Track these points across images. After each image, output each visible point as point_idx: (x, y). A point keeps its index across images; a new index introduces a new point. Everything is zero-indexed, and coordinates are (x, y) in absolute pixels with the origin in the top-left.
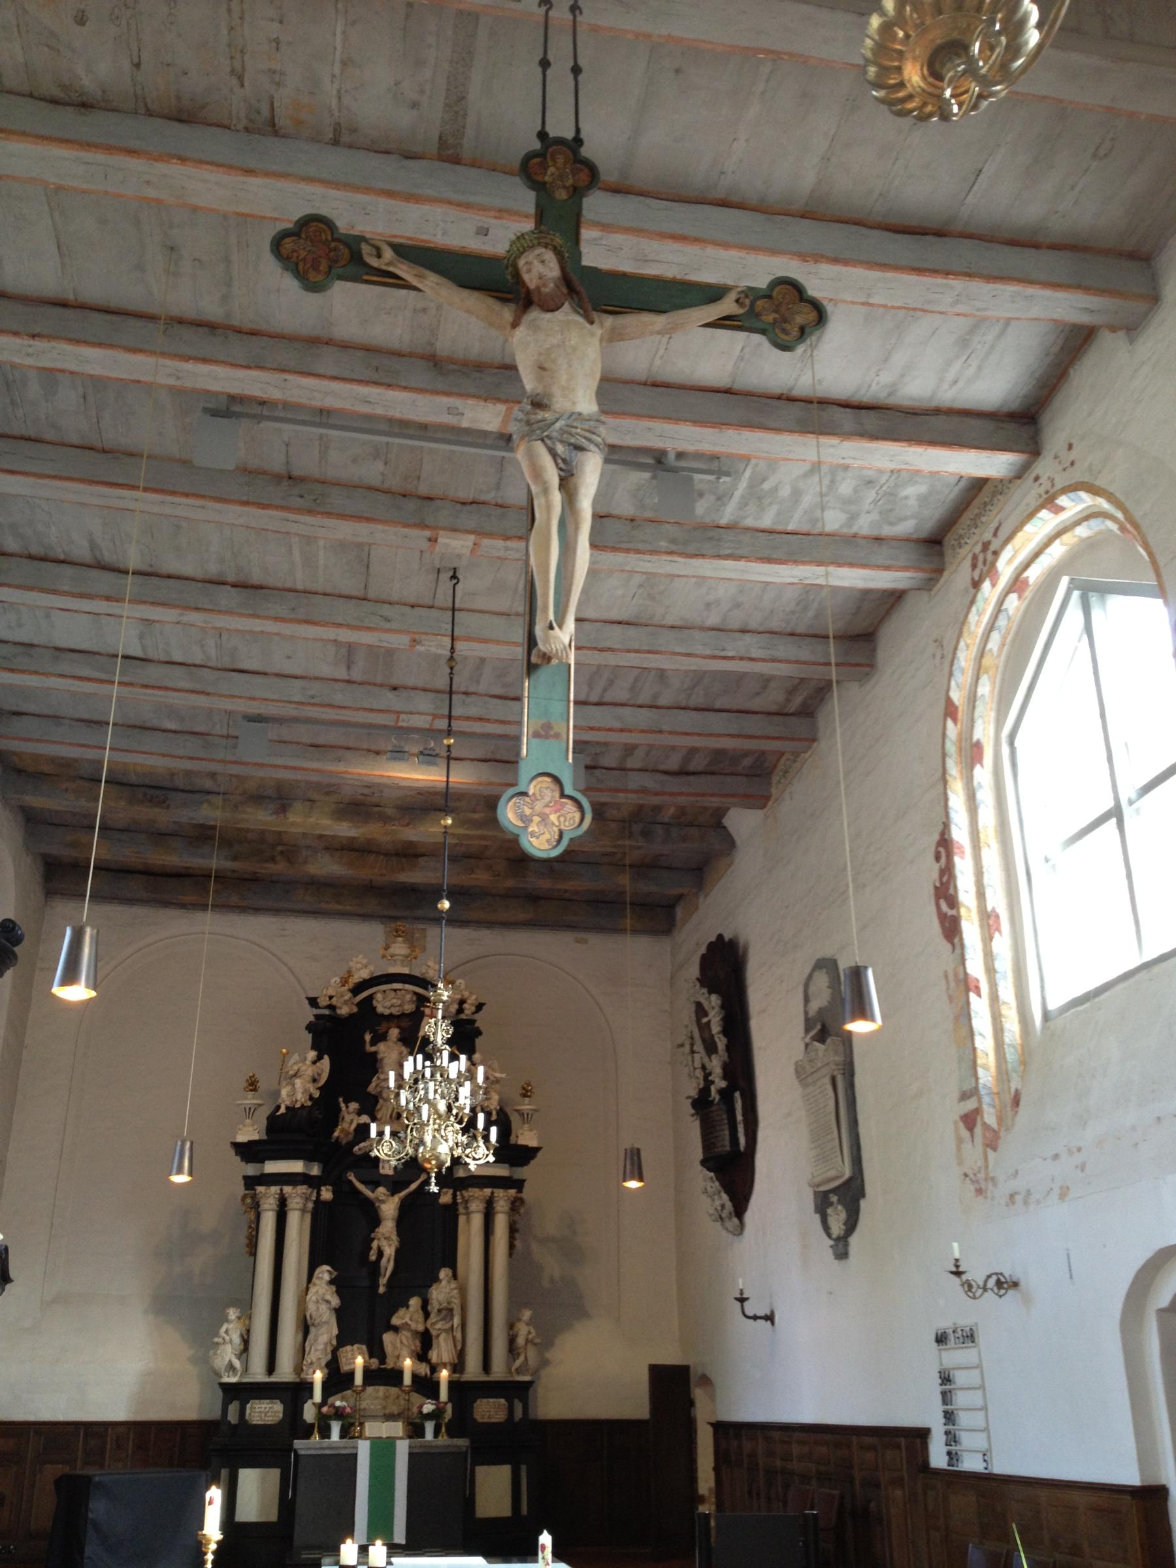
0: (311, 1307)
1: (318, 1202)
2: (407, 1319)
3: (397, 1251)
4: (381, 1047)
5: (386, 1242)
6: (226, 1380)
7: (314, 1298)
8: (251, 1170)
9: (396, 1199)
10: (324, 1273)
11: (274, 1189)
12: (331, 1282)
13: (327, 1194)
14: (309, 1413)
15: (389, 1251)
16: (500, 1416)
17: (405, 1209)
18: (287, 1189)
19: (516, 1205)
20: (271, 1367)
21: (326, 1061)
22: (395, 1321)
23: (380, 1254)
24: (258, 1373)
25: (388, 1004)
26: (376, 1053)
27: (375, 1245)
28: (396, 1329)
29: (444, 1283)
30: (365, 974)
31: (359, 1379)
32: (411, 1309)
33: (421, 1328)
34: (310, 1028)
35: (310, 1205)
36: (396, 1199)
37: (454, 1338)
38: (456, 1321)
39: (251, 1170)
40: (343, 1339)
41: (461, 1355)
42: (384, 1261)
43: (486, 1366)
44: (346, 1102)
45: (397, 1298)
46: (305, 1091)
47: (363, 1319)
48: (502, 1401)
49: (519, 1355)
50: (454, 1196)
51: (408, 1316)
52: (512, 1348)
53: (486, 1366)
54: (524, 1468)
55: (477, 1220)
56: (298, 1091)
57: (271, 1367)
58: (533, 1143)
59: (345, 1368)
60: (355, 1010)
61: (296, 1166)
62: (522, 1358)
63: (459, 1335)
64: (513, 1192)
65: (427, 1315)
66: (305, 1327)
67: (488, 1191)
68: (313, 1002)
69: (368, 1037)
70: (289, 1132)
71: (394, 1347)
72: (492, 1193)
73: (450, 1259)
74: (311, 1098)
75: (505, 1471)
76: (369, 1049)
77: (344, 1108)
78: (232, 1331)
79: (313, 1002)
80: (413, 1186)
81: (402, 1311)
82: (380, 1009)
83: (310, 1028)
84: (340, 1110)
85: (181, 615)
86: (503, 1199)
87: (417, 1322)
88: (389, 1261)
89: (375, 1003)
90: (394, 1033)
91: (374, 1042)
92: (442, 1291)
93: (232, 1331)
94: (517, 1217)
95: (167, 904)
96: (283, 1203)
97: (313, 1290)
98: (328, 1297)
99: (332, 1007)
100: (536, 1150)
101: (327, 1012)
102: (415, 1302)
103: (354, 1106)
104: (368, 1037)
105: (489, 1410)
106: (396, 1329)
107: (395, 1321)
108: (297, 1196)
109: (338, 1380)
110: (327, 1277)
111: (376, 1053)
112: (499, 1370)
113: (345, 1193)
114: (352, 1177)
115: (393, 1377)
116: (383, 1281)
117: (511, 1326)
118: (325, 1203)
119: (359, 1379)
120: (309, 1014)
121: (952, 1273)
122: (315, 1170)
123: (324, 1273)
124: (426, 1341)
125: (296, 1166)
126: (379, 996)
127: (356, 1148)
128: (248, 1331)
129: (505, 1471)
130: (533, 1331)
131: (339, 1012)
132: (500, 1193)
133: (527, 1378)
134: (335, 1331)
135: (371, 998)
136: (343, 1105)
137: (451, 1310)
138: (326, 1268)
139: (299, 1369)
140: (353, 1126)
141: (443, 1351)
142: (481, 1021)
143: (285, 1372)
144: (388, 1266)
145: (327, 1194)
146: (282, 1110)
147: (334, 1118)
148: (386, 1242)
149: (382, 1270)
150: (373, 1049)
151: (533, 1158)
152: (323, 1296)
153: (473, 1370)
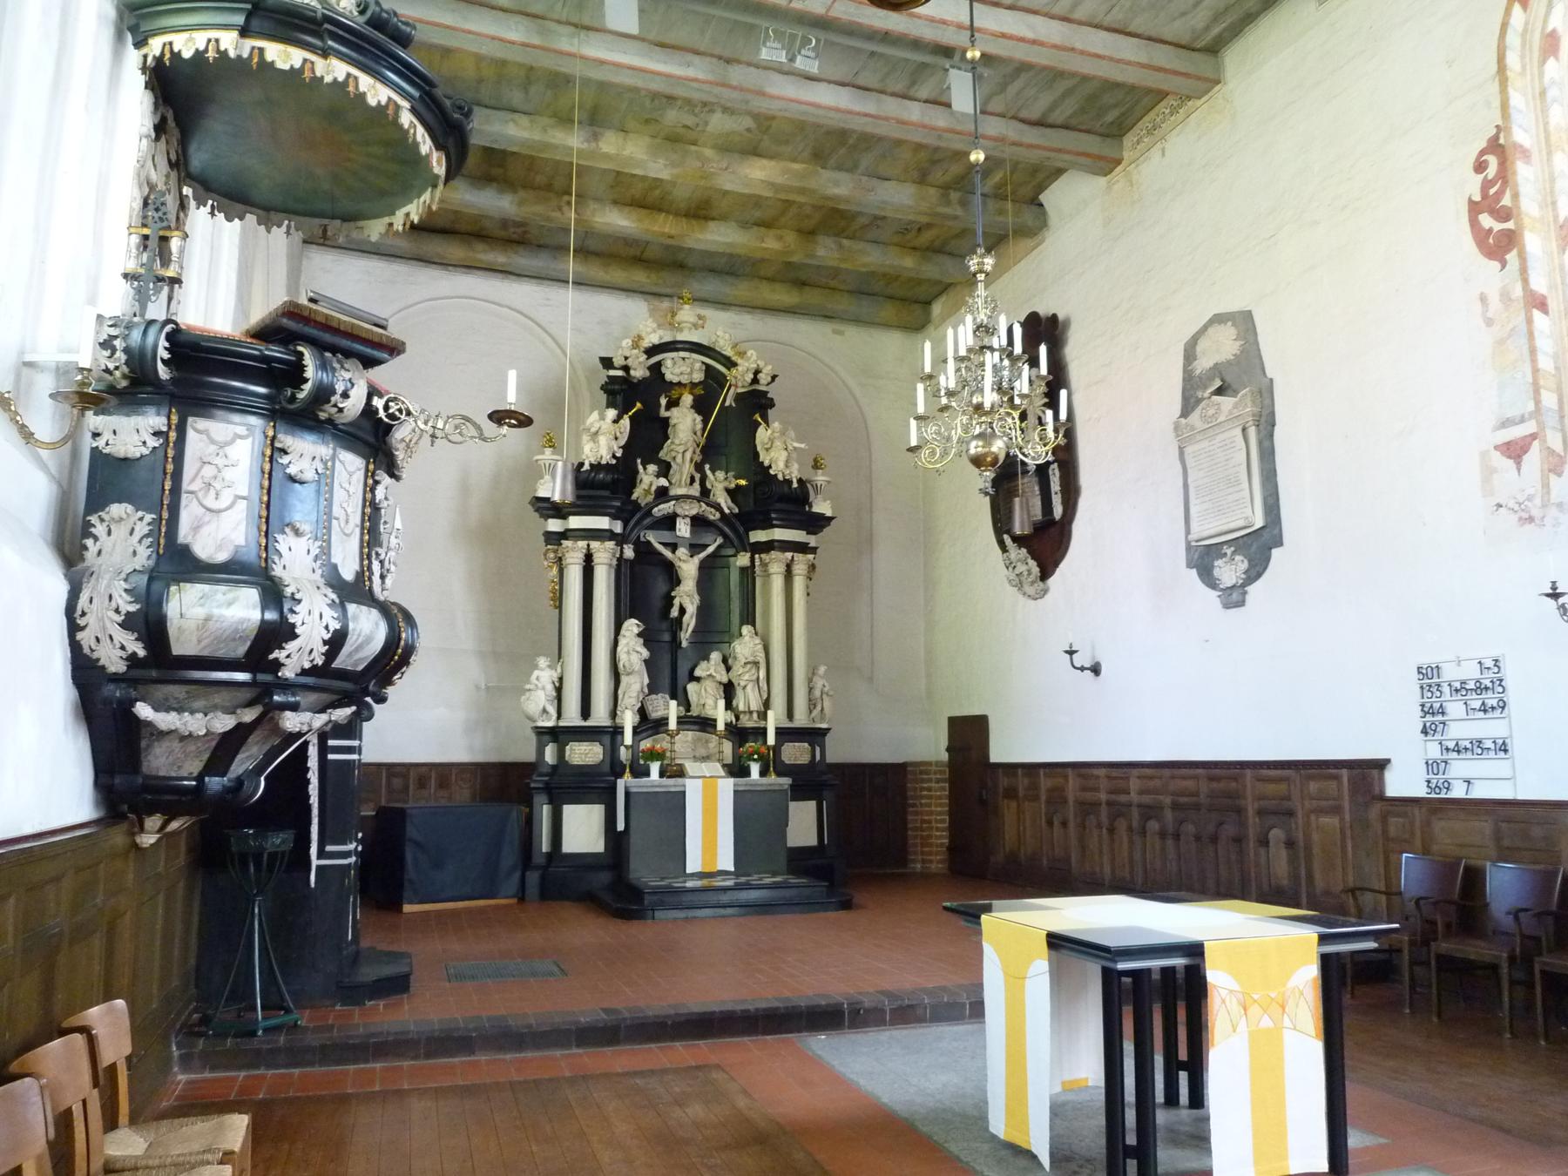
1: (620, 559)
2: (712, 671)
3: (699, 609)
4: (675, 412)
5: (687, 597)
6: (540, 724)
8: (554, 525)
9: (696, 560)
10: (632, 626)
11: (582, 544)
12: (639, 635)
13: (629, 552)
14: (624, 754)
15: (691, 609)
16: (804, 759)
17: (704, 567)
18: (595, 545)
19: (812, 567)
20: (586, 711)
22: (698, 673)
23: (682, 611)
24: (572, 717)
25: (677, 371)
26: (667, 419)
27: (676, 602)
28: (698, 679)
31: (673, 725)
33: (725, 680)
35: (615, 562)
36: (696, 560)
39: (554, 525)
40: (653, 688)
42: (686, 618)
47: (669, 673)
50: (752, 560)
51: (711, 668)
55: (777, 583)
57: (586, 711)
58: (829, 513)
59: (655, 714)
60: (648, 374)
61: (602, 522)
64: (811, 556)
65: (728, 669)
67: (789, 555)
68: (607, 363)
69: (663, 401)
71: (699, 694)
73: (749, 617)
74: (614, 456)
75: (812, 805)
76: (663, 413)
78: (544, 676)
80: (711, 549)
81: (703, 664)
82: (669, 377)
84: (637, 472)
86: (801, 563)
89: (663, 370)
90: (687, 399)
91: (668, 408)
92: (746, 646)
93: (544, 676)
96: (589, 558)
97: (622, 642)
99: (626, 368)
100: (831, 519)
101: (620, 373)
102: (715, 656)
103: (652, 468)
104: (663, 401)
105: (796, 753)
106: (698, 679)
107: (698, 673)
109: (649, 725)
110: (636, 630)
111: (667, 419)
112: (801, 720)
113: (644, 550)
115: (706, 724)
117: (810, 680)
119: (673, 725)
120: (603, 375)
121: (1548, 595)
122: (618, 527)
123: (632, 626)
124: (729, 690)
125: (602, 522)
126: (669, 363)
128: (561, 679)
129: (812, 805)
132: (799, 557)
133: (824, 726)
134: (646, 681)
135: (659, 364)
140: (654, 488)
141: (748, 699)
143: (600, 717)
144: (690, 621)
146: (586, 467)
147: (632, 480)
148: (687, 597)
150: (667, 414)
151: (823, 527)
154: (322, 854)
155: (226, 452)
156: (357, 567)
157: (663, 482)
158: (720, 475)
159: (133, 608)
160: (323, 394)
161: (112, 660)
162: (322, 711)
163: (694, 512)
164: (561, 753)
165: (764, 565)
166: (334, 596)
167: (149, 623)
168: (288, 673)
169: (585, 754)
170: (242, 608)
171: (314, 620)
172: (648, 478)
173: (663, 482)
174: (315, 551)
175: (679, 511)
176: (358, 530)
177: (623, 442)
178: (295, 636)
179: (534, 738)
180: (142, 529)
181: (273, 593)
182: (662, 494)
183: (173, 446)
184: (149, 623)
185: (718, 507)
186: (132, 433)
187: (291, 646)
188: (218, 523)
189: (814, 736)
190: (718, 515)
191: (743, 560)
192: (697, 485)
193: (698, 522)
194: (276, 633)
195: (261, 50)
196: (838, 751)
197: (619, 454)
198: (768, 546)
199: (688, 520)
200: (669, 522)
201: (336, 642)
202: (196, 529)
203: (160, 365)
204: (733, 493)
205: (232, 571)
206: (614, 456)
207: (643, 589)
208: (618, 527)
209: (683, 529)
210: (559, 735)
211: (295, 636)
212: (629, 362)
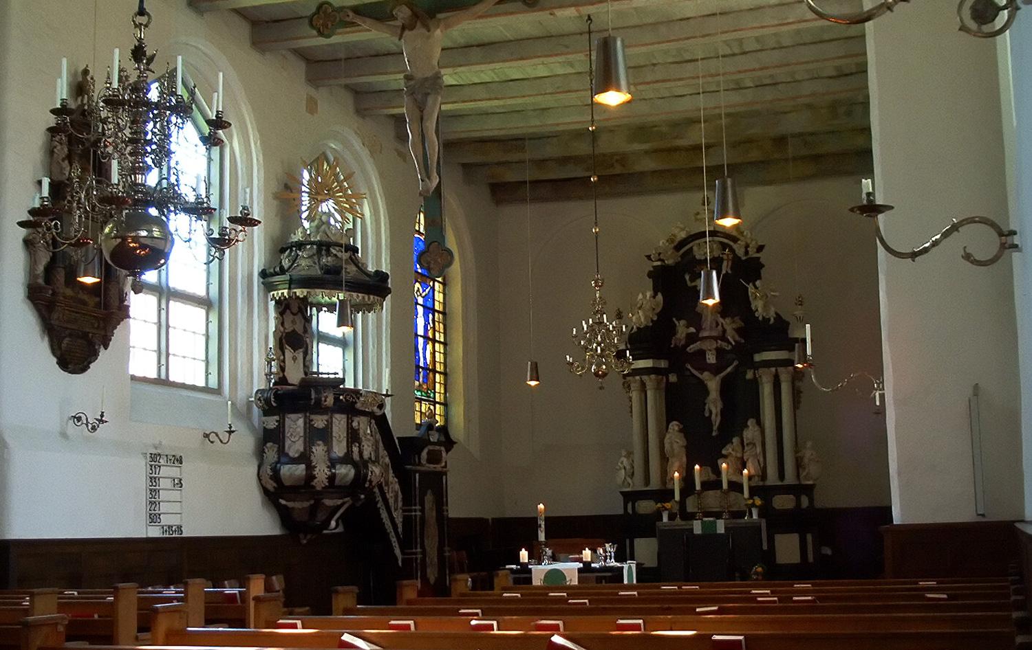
0: (667, 446)
7: (669, 441)
10: (674, 426)
18: (645, 378)
21: (660, 297)
22: (724, 452)
23: (711, 412)
24: (637, 485)
27: (707, 407)
29: (751, 427)
30: (683, 235)
32: (734, 444)
33: (739, 455)
34: (650, 275)
35: (663, 385)
37: (759, 461)
38: (759, 449)
41: (764, 470)
43: (782, 475)
44: (679, 320)
45: (725, 438)
46: (646, 317)
48: (792, 496)
49: (805, 468)
50: (754, 374)
52: (799, 464)
53: (782, 475)
54: (809, 537)
56: (639, 319)
60: (679, 259)
62: (807, 471)
63: (761, 460)
66: (664, 459)
67: (773, 369)
70: (641, 342)
72: (776, 370)
73: (757, 415)
74: (652, 321)
77: (678, 324)
79: (649, 257)
83: (650, 275)
84: (676, 325)
85: (454, 70)
87: (737, 452)
88: (716, 415)
91: (692, 280)
92: (751, 432)
94: (798, 384)
95: (569, 198)
96: (643, 384)
98: (679, 441)
101: (659, 263)
102: (736, 440)
103: (683, 322)
104: (687, 277)
105: (783, 502)
107: (724, 452)
108: (650, 380)
110: (676, 428)
112: (790, 479)
114: (689, 367)
116: (715, 428)
118: (672, 384)
120: (649, 266)
122: (663, 364)
123: (674, 426)
126: (695, 248)
127: (688, 349)
130: (814, 453)
131: (666, 262)
132: (781, 370)
136: (676, 322)
137: (754, 444)
138: (675, 422)
139: (664, 482)
142: (763, 256)
143: (655, 484)
144: (716, 420)
145: (673, 378)
147: (673, 330)
148: (714, 406)
149: (714, 423)
150: (693, 284)
152: (675, 439)
153: (772, 479)
154: (403, 553)
155: (296, 424)
156: (346, 451)
157: (692, 330)
158: (728, 320)
159: (271, 474)
160: (318, 401)
161: (272, 489)
162: (342, 499)
163: (715, 346)
164: (633, 507)
165: (760, 377)
166: (329, 464)
167: (276, 476)
168: (319, 488)
169: (645, 507)
170: (300, 469)
171: (322, 473)
172: (682, 329)
173: (692, 330)
174: (325, 449)
175: (704, 348)
176: (345, 439)
177: (658, 310)
178: (316, 478)
179: (621, 498)
180: (276, 450)
181: (310, 467)
182: (692, 339)
183: (281, 424)
184: (276, 476)
185: (729, 343)
186: (272, 422)
187: (316, 481)
188: (295, 446)
189: (798, 490)
190: (730, 346)
191: (749, 375)
192: (720, 327)
193: (720, 352)
194: (310, 477)
195: (295, 293)
196: (825, 500)
197: (655, 319)
198: (767, 364)
199: (714, 352)
200: (702, 353)
201: (332, 478)
202: (289, 448)
203: (273, 402)
204: (738, 330)
205: (294, 461)
206: (652, 321)
207: (680, 403)
208: (663, 364)
209: (711, 359)
210: (630, 497)
211: (316, 478)
212: (662, 257)
